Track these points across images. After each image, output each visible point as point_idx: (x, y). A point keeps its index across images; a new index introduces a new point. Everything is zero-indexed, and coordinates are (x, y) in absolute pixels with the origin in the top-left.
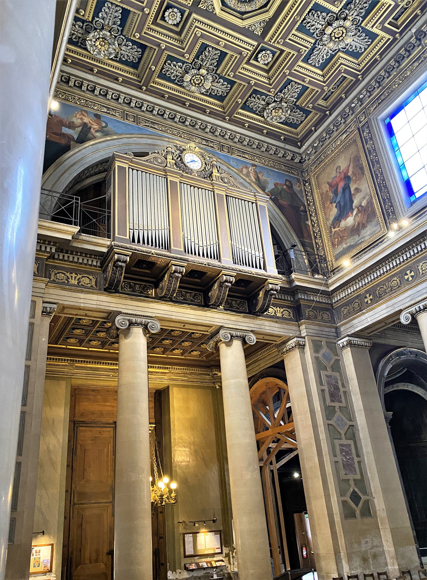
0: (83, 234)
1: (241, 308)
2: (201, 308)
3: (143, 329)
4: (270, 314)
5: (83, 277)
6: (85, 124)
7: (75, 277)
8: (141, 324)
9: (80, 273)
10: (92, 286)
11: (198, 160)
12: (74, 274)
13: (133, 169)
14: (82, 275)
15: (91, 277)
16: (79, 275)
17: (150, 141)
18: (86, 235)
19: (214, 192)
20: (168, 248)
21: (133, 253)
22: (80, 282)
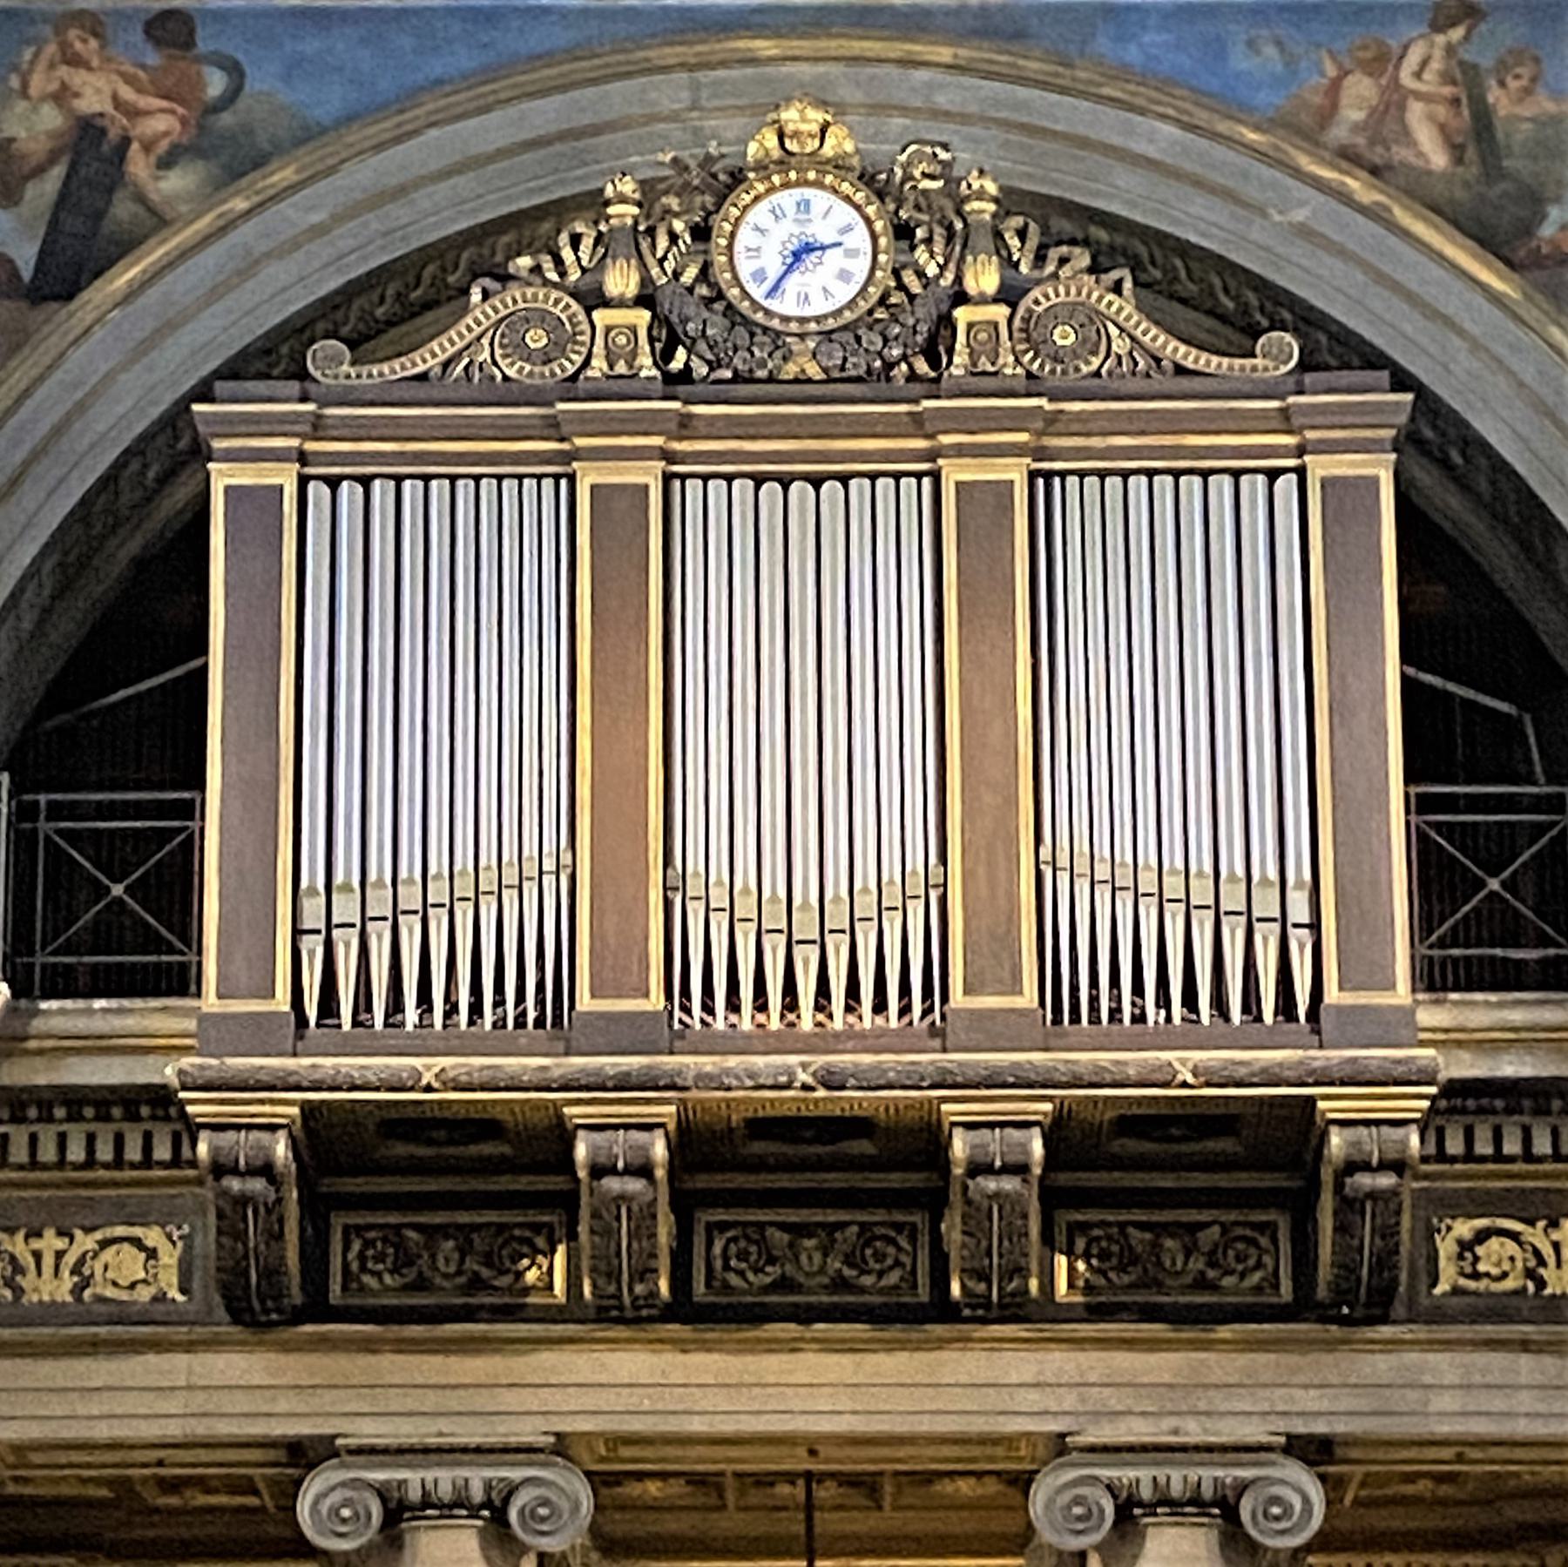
0: (44, 1005)
1: (1228, 1281)
2: (895, 1332)
3: (482, 1532)
4: (1482, 1285)
5: (105, 1244)
6: (88, 130)
7: (60, 1255)
8: (457, 1505)
9: (87, 1223)
10: (160, 1298)
11: (848, 229)
12: (49, 1233)
13: (333, 483)
14: (98, 1235)
15: (153, 1236)
16: (78, 1233)
17: (545, 114)
18: (69, 1004)
19: (936, 476)
20: (555, 1018)
21: (308, 1109)
22: (86, 1283)
